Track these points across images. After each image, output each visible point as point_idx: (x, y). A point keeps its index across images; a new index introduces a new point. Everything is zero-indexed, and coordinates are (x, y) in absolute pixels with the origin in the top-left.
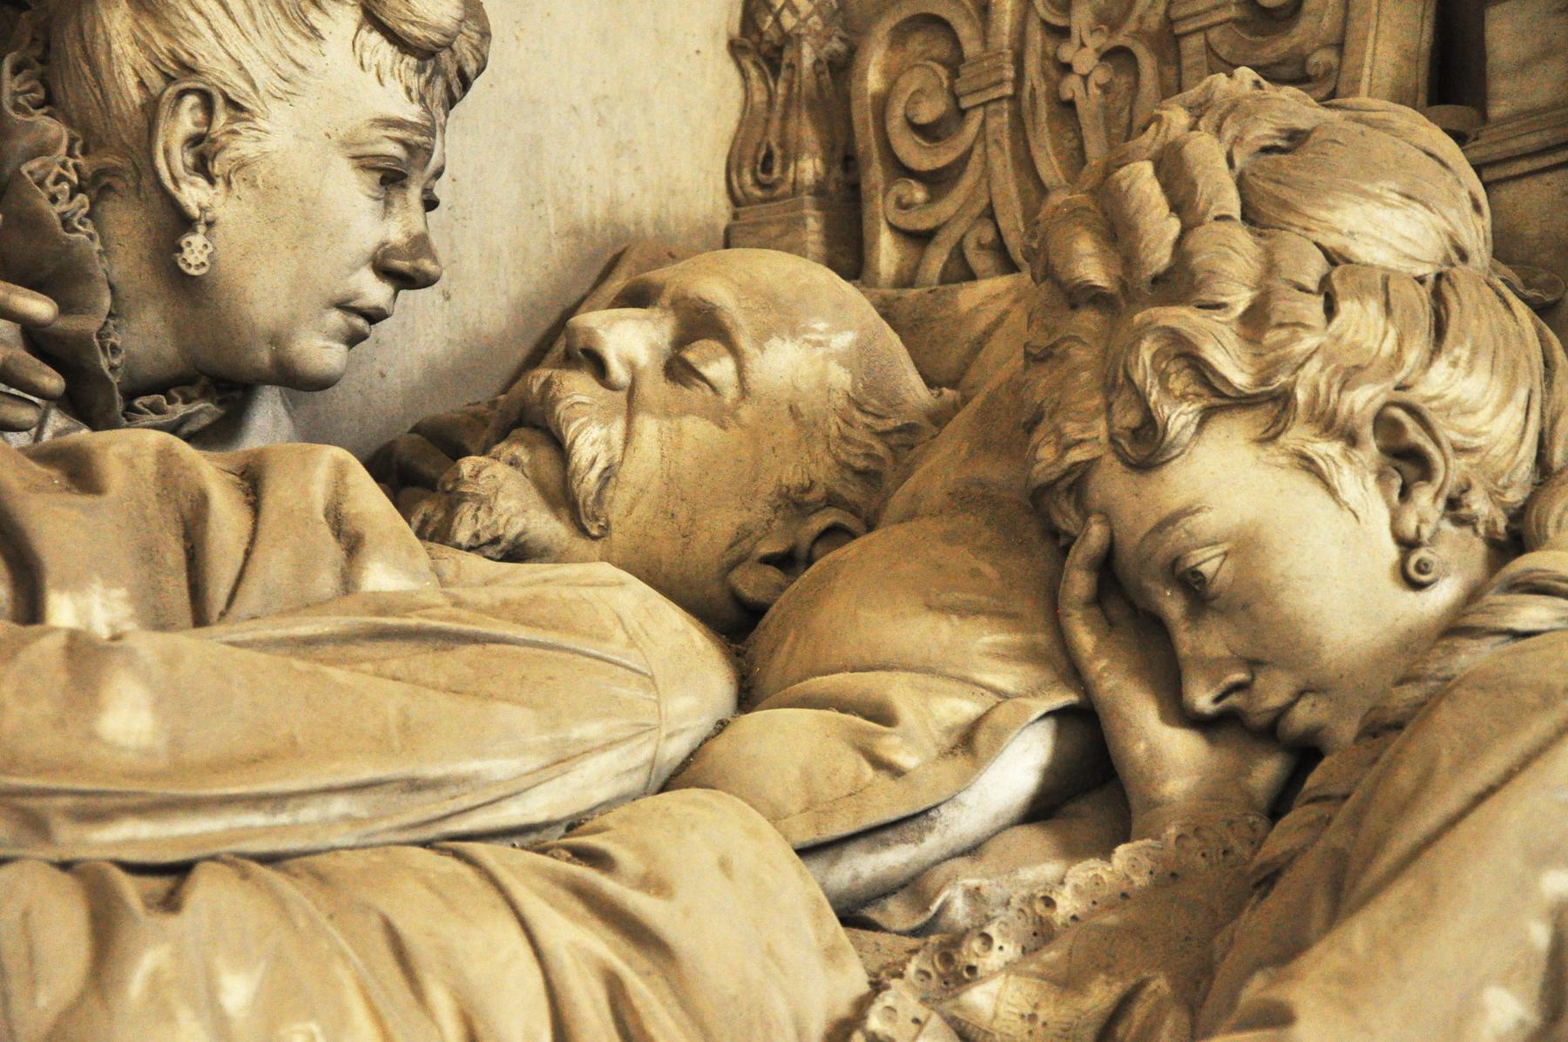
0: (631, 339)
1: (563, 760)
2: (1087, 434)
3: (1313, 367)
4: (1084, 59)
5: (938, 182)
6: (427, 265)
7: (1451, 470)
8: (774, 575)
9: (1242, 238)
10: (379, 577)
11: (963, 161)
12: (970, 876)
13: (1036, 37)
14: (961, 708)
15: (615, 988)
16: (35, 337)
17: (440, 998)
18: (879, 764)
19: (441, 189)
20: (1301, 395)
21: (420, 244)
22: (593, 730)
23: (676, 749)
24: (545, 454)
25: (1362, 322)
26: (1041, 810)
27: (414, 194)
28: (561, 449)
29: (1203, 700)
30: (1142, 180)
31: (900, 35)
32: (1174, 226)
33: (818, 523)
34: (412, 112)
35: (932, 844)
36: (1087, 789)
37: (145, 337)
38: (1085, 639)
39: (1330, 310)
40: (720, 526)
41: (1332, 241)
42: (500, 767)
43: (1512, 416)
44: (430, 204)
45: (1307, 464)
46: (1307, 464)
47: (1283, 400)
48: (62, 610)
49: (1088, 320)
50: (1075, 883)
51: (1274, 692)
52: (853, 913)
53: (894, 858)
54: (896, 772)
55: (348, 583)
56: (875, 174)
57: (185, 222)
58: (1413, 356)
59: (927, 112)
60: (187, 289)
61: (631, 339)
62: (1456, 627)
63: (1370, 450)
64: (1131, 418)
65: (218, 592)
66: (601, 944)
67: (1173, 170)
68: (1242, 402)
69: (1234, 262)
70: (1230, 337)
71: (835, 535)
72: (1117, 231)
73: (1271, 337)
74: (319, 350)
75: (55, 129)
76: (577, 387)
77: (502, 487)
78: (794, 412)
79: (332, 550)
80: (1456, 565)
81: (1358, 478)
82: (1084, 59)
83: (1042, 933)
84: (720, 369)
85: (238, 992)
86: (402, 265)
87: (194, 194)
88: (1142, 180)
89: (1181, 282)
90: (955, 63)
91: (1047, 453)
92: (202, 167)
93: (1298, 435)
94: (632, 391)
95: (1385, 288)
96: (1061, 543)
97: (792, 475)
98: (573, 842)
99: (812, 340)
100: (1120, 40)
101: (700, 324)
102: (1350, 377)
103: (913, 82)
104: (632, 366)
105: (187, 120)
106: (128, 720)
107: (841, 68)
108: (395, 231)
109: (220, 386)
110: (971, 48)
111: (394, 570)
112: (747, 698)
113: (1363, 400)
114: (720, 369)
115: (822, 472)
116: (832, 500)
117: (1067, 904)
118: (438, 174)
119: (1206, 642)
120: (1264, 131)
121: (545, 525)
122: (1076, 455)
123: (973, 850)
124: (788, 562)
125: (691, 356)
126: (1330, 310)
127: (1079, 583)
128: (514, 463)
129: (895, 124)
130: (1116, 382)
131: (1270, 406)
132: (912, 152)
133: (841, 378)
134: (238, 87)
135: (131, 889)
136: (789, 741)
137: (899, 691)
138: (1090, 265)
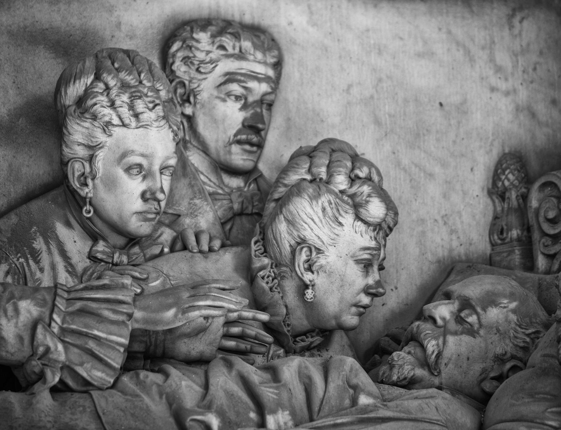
10: (364, 400)
21: (378, 284)
24: (418, 351)
34: (373, 244)
56: (536, 235)
57: (306, 287)
59: (551, 215)
65: (316, 408)
71: (515, 369)
74: (351, 320)
75: (266, 261)
87: (308, 277)
92: (310, 269)
103: (545, 206)
105: (303, 256)
107: (525, 198)
108: (371, 281)
124: (500, 378)
134: (318, 244)
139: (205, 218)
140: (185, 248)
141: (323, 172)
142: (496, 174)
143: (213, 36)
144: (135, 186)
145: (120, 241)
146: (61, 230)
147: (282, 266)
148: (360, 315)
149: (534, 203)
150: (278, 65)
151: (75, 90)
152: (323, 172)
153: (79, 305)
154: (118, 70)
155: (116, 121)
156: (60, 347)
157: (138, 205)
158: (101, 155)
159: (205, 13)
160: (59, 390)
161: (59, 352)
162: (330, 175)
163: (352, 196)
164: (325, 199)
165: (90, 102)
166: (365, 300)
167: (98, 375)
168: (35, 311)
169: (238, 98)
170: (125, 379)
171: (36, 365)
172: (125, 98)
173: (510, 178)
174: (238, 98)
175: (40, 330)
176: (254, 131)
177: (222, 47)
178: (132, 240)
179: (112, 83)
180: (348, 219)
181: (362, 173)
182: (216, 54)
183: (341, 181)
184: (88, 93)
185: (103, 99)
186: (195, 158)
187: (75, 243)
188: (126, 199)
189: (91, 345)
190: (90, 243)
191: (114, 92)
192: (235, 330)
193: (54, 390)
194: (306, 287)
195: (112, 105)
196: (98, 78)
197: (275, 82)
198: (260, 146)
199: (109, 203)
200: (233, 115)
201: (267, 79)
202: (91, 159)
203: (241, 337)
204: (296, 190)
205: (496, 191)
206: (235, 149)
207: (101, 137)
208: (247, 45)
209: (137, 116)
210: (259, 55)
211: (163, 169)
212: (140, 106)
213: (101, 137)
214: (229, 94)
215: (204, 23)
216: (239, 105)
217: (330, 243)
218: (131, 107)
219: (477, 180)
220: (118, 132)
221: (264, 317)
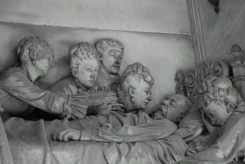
0: (167, 102)
1: (163, 133)
2: (202, 104)
3: (218, 97)
4: (202, 77)
5: (192, 88)
6: (151, 98)
7: (230, 103)
8: (180, 119)
9: (212, 88)
10: (148, 121)
11: (194, 86)
12: (197, 139)
13: (198, 76)
14: (194, 127)
15: (168, 149)
16: (122, 108)
17: (155, 151)
18: (188, 131)
19: (151, 93)
20: (218, 99)
21: (150, 97)
22: (166, 131)
23: (173, 132)
24: (161, 112)
25: (222, 93)
26: (202, 134)
27: (149, 93)
28: (162, 111)
29: (213, 123)
30: (204, 84)
31: (188, 77)
32: (206, 87)
33: (184, 115)
34: (148, 87)
35: (193, 137)
36: (205, 132)
38: (204, 120)
39: (219, 92)
40: (176, 116)
41: (219, 87)
42: (159, 134)
43: (235, 99)
44: (151, 94)
45: (219, 104)
46: (219, 104)
47: (216, 99)
48: (125, 125)
49: (201, 95)
50: (204, 138)
51: (219, 122)
52: (187, 143)
53: (190, 139)
54: (190, 132)
55: (146, 122)
56: (187, 88)
57: (132, 97)
58: (226, 95)
59: (191, 83)
60: (132, 102)
61: (167, 102)
62: (231, 115)
63: (224, 103)
64: (205, 102)
65: (136, 123)
66: (167, 146)
67: (206, 83)
68: (213, 100)
69: (211, 90)
70: (212, 95)
71: (185, 116)
72: (202, 89)
73: (215, 95)
74: (143, 106)
75: (122, 92)
76: (163, 106)
77: (158, 115)
78: (181, 106)
79: (144, 120)
80: (231, 110)
81: (223, 105)
82: (202, 77)
83: (202, 142)
84: (174, 104)
85: (140, 151)
86: (149, 99)
87: (132, 95)
88: (204, 84)
89: (207, 92)
90: (192, 79)
91: (199, 106)
92: (133, 93)
93: (218, 102)
94: (167, 106)
95: (223, 90)
96: (201, 113)
97: (181, 111)
98: (165, 139)
99: (181, 101)
100: (205, 75)
101: (173, 100)
102: (221, 97)
103: (189, 80)
104: (167, 104)
107: (184, 80)
108: (148, 96)
109: (136, 110)
110: (194, 77)
111: (149, 121)
112: (178, 128)
113: (222, 99)
114: (174, 104)
115: (184, 111)
116: (185, 113)
117: (203, 140)
118: (151, 92)
119: (213, 119)
120: (213, 79)
121: (162, 117)
122: (201, 106)
123: (197, 138)
124: (181, 118)
125: (172, 103)
126: (219, 92)
127: (203, 116)
128: (159, 113)
129: (188, 84)
130: (203, 100)
132: (190, 86)
133: (184, 103)
134: (135, 87)
135: (131, 144)
136: (182, 132)
137: (189, 126)
138: (201, 91)
139: (106, 84)
140: (101, 90)
141: (135, 69)
142: (176, 76)
143: (107, 42)
144: (88, 74)
145: (85, 89)
146: (70, 86)
147: (126, 93)
148: (146, 105)
149: (186, 81)
150: (122, 49)
151: (73, 51)
152: (135, 69)
153: (75, 99)
154: (84, 46)
155: (83, 58)
156: (70, 109)
157: (89, 79)
158: (80, 66)
159: (105, 38)
161: (70, 110)
162: (137, 70)
163: (143, 75)
164: (136, 76)
165: (77, 53)
166: (147, 101)
167: (81, 116)
168: (64, 100)
169: (113, 56)
170: (87, 117)
171: (64, 114)
172: (86, 52)
173: (180, 76)
174: (113, 56)
175: (65, 104)
176: (117, 64)
177: (109, 44)
179: (82, 48)
180: (142, 81)
181: (145, 70)
182: (108, 46)
183: (140, 71)
184: (76, 51)
185: (80, 52)
186: (103, 71)
187: (74, 89)
188: (85, 77)
189: (78, 108)
190: (77, 89)
191: (83, 51)
192: (114, 109)
193: (69, 120)
194: (132, 97)
195: (83, 54)
196: (79, 47)
197: (123, 53)
198: (119, 68)
200: (112, 60)
201: (120, 52)
202: (77, 67)
203: (116, 110)
204: (129, 74)
205: (177, 79)
206: (113, 68)
207: (80, 62)
208: (115, 43)
209: (88, 56)
210: (118, 46)
211: (95, 70)
212: (89, 54)
213: (80, 62)
214: (111, 55)
215: (104, 40)
216: (113, 58)
217: (138, 87)
218: (87, 54)
219: (173, 77)
220: (84, 60)
221: (122, 105)
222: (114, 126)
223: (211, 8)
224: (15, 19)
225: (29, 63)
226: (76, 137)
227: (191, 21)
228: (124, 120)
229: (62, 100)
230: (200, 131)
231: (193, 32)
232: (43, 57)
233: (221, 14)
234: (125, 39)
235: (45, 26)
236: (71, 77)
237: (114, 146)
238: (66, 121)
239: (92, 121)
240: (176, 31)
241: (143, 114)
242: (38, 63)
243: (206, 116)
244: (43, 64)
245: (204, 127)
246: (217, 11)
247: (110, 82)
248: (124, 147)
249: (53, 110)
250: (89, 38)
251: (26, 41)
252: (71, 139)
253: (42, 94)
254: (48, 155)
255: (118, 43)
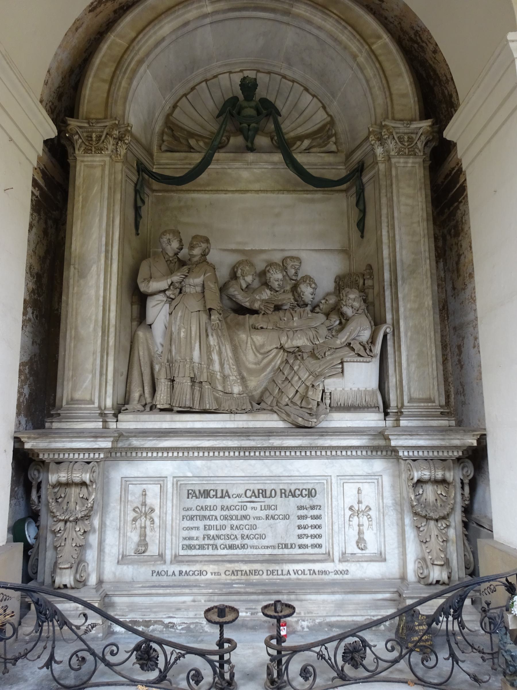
0: (323, 301)
25: (350, 301)
36: (340, 323)
37: (302, 303)
61: (323, 301)
69: (345, 298)
77: (317, 310)
81: (350, 308)
89: (342, 300)
95: (351, 299)
98: (315, 328)
99: (332, 300)
101: (327, 300)
106: (295, 324)
131: (346, 305)
139: (288, 288)
144: (277, 283)
147: (299, 296)
150: (300, 263)
151: (268, 269)
160: (264, 314)
167: (270, 312)
173: (337, 280)
176: (296, 274)
178: (277, 291)
187: (268, 292)
188: (276, 285)
197: (300, 266)
199: (273, 286)
200: (293, 271)
204: (301, 283)
205: (335, 282)
217: (306, 291)
219: (333, 280)
222: (288, 319)
223: (359, 234)
224: (233, 247)
225: (241, 278)
226: (265, 327)
227: (349, 239)
228: (294, 315)
229: (259, 303)
230: (338, 322)
231: (350, 247)
232: (249, 274)
233: (365, 239)
234: (303, 255)
235: (252, 250)
236: (266, 284)
237: (285, 333)
238: (261, 315)
239: (275, 317)
240: (338, 247)
241: (309, 308)
242: (246, 278)
243: (342, 315)
244: (249, 279)
245: (340, 320)
246: (362, 237)
247: (291, 286)
248: (291, 333)
249: (254, 308)
250: (277, 257)
251: (239, 263)
252: (262, 328)
253: (248, 299)
254: (249, 338)
255: (298, 259)
